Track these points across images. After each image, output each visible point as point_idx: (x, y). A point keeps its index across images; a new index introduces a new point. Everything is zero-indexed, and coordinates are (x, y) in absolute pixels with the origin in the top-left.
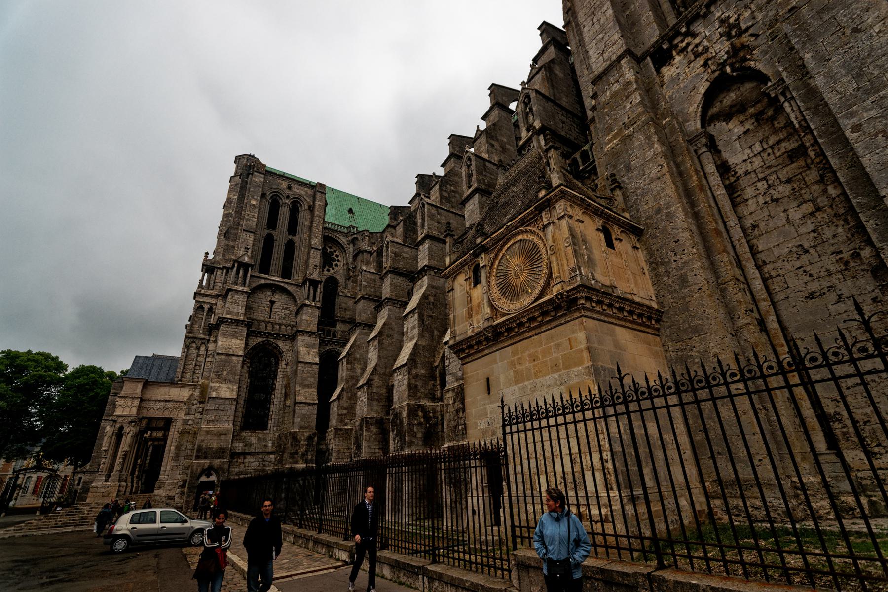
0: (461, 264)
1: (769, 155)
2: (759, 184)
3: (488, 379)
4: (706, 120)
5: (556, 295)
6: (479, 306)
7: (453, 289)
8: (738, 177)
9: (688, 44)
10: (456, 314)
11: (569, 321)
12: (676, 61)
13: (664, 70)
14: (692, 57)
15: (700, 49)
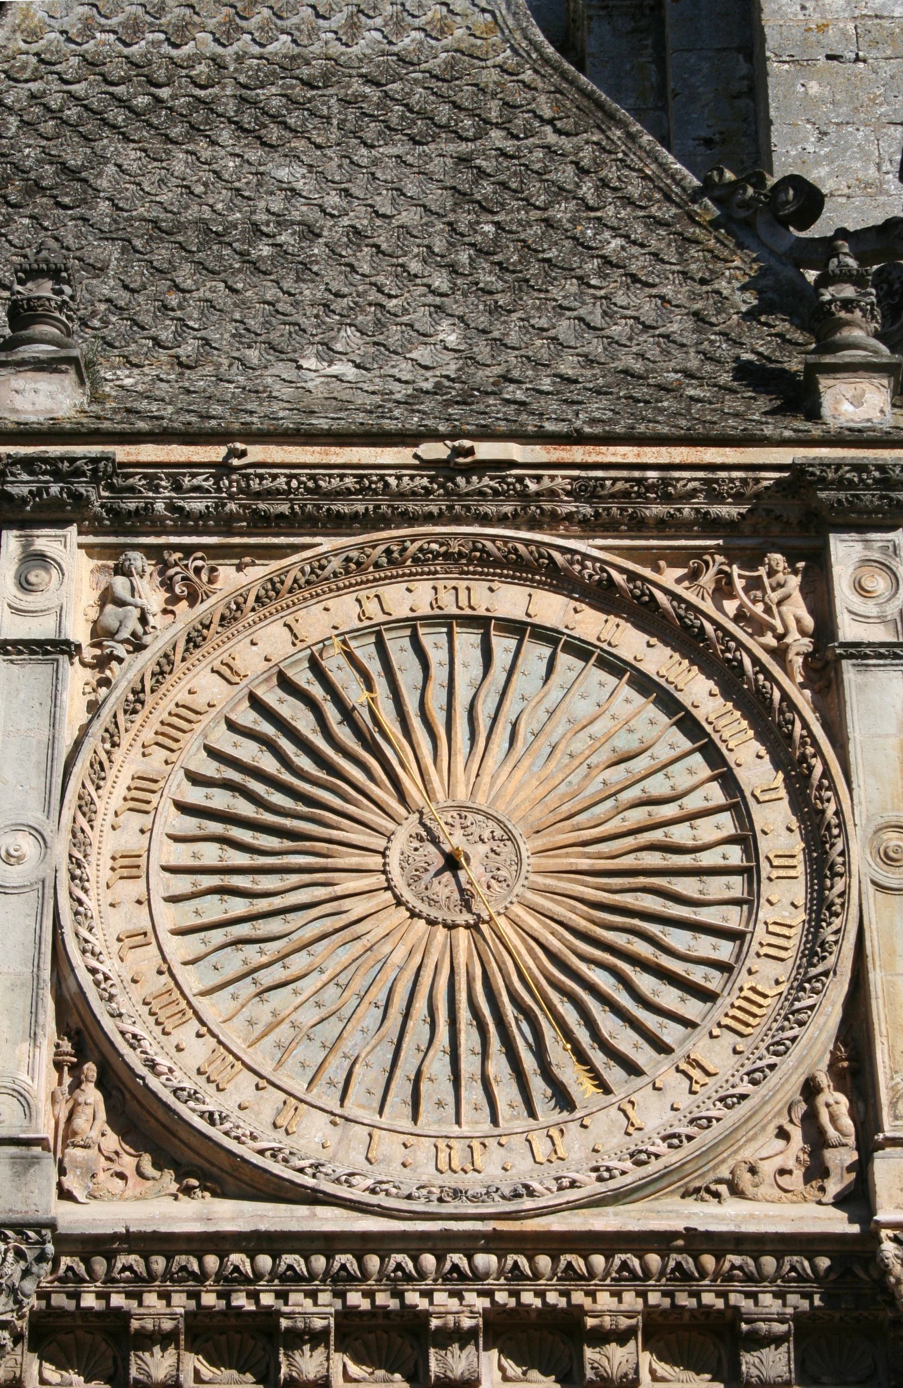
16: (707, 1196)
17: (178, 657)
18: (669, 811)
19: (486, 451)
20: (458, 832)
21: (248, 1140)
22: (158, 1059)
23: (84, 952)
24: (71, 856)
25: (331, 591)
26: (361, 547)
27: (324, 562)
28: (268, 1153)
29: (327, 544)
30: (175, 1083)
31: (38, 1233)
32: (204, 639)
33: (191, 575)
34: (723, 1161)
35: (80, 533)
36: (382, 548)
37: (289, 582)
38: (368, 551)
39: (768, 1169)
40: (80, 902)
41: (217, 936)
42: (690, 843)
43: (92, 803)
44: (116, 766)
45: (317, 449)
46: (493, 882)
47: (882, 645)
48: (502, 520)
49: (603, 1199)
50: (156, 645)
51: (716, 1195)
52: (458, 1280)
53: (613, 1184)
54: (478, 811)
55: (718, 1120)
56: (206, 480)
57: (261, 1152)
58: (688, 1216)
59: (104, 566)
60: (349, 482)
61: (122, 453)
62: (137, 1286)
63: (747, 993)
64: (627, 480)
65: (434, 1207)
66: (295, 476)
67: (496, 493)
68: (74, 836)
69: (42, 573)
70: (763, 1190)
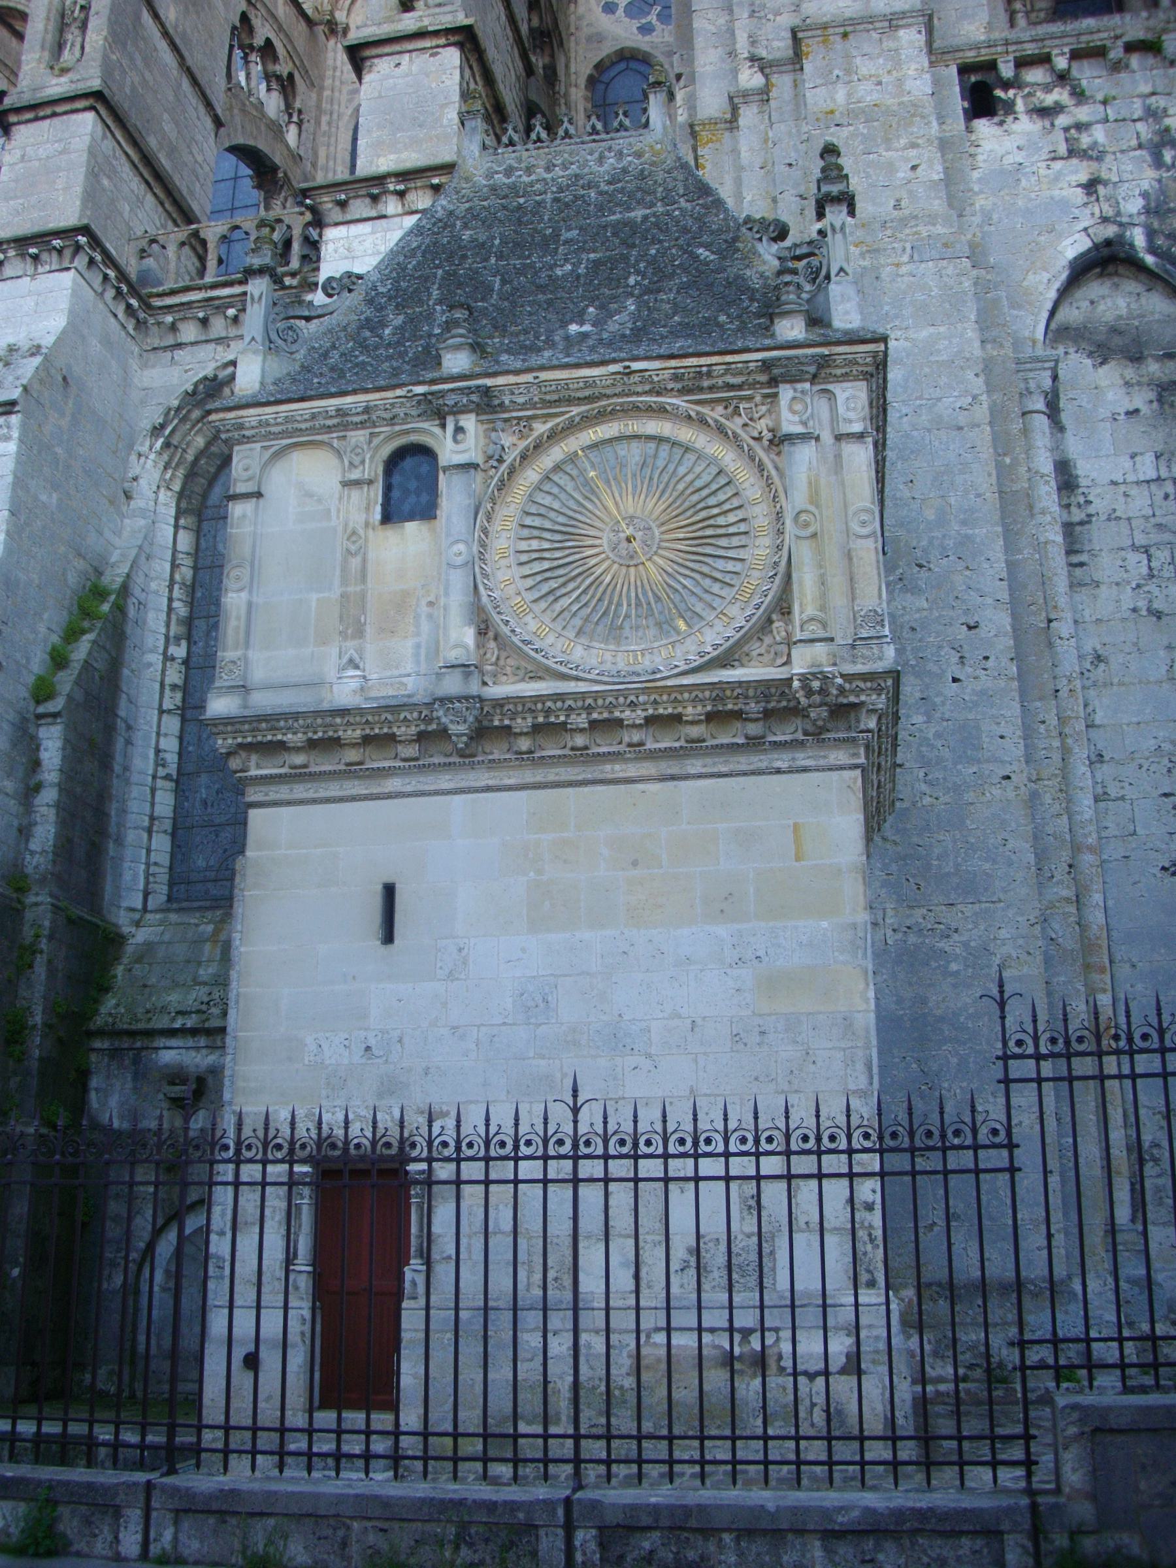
0: (341, 413)
1: (1166, 497)
2: (1133, 558)
3: (389, 891)
4: (1058, 334)
5: (804, 678)
6: (402, 602)
7: (259, 495)
8: (1089, 516)
9: (1058, 109)
10: (258, 599)
11: (805, 770)
12: (1016, 127)
13: (983, 126)
14: (1062, 149)
15: (1085, 140)
18: (715, 511)
19: (636, 366)
29: (575, 410)
39: (754, 653)
41: (539, 578)
48: (645, 393)
50: (509, 459)
61: (489, 382)
62: (514, 716)
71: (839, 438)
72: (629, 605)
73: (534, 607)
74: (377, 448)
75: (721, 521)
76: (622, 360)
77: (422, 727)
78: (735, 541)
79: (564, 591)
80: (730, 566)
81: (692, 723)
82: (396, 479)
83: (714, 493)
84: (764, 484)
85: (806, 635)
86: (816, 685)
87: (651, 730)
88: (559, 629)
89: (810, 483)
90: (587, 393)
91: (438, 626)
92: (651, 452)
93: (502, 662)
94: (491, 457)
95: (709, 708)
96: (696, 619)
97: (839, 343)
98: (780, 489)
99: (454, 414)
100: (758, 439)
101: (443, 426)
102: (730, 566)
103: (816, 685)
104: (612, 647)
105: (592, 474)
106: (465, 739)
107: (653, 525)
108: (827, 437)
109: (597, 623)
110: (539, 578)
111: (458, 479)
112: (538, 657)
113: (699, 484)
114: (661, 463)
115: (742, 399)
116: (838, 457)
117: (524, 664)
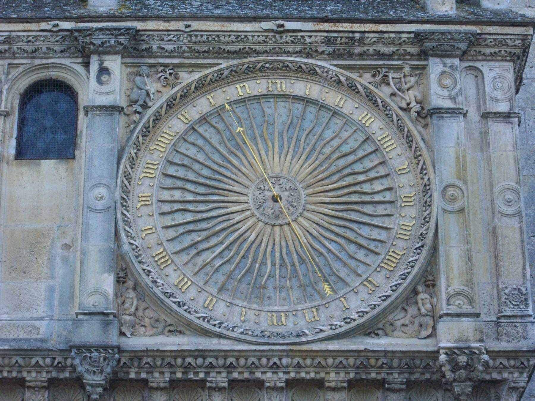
5: (451, 353)
16: (373, 335)
17: (163, 113)
18: (362, 178)
19: (290, 25)
20: (277, 187)
21: (194, 313)
22: (158, 280)
23: (128, 237)
24: (121, 197)
25: (226, 84)
26: (237, 66)
27: (222, 72)
28: (201, 319)
29: (224, 64)
30: (165, 290)
31: (112, 350)
32: (174, 105)
33: (168, 76)
34: (380, 322)
35: (123, 57)
36: (246, 66)
37: (208, 80)
38: (240, 67)
39: (398, 323)
40: (126, 216)
41: (181, 230)
42: (370, 191)
43: (130, 174)
44: (139, 159)
45: (219, 23)
46: (290, 207)
47: (450, 109)
49: (333, 337)
50: (155, 106)
51: (377, 335)
52: (275, 367)
53: (337, 331)
54: (284, 178)
55: (379, 305)
56: (174, 37)
57: (199, 318)
58: (366, 344)
59: (132, 72)
60: (233, 38)
61: (139, 25)
63: (391, 253)
64: (347, 38)
65: (266, 341)
66: (210, 35)
67: (293, 42)
68: (123, 189)
69: (107, 77)
70: (396, 333)
71: (486, 116)
72: (273, 265)
73: (175, 258)
74: (15, 80)
75: (366, 188)
76: (276, 18)
77: (54, 374)
78: (381, 209)
79: (206, 245)
80: (375, 234)
81: (334, 389)
82: (31, 113)
83: (360, 160)
84: (412, 155)
85: (453, 309)
86: (463, 359)
87: (290, 394)
88: (201, 284)
89: (458, 158)
90: (237, 47)
91: (73, 271)
92: (298, 113)
93: (140, 313)
94: (135, 102)
95: (352, 375)
96: (340, 284)
97: (490, 23)
98: (429, 162)
99: (99, 53)
100: (407, 110)
101: (87, 65)
102: (375, 234)
103: (463, 359)
104: (254, 306)
105: (239, 129)
106: (100, 390)
107: (300, 187)
108: (474, 115)
109: (240, 281)
110: (181, 230)
111: (101, 122)
112: (181, 310)
113: (345, 149)
114: (308, 125)
115: (390, 68)
116: (484, 135)
117: (163, 316)
